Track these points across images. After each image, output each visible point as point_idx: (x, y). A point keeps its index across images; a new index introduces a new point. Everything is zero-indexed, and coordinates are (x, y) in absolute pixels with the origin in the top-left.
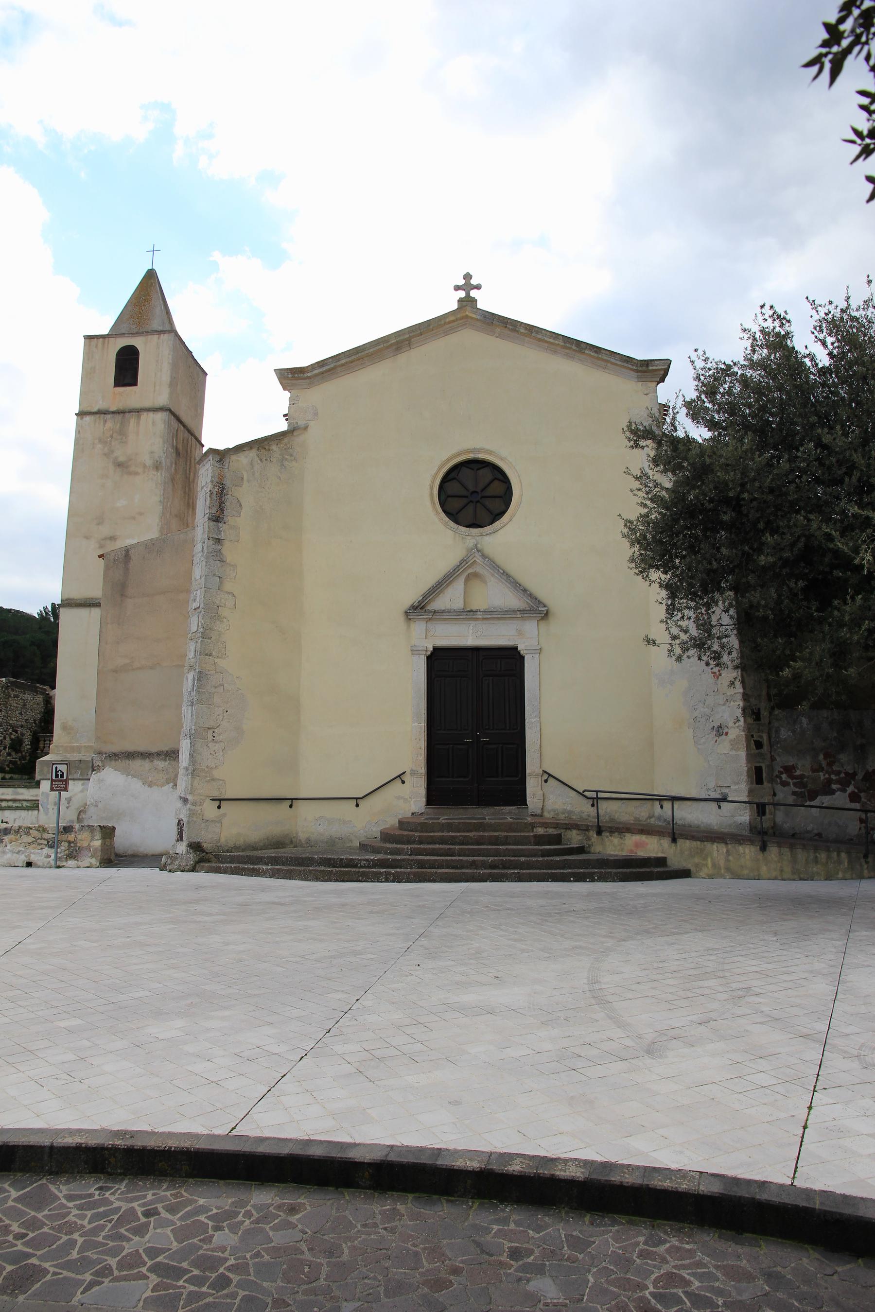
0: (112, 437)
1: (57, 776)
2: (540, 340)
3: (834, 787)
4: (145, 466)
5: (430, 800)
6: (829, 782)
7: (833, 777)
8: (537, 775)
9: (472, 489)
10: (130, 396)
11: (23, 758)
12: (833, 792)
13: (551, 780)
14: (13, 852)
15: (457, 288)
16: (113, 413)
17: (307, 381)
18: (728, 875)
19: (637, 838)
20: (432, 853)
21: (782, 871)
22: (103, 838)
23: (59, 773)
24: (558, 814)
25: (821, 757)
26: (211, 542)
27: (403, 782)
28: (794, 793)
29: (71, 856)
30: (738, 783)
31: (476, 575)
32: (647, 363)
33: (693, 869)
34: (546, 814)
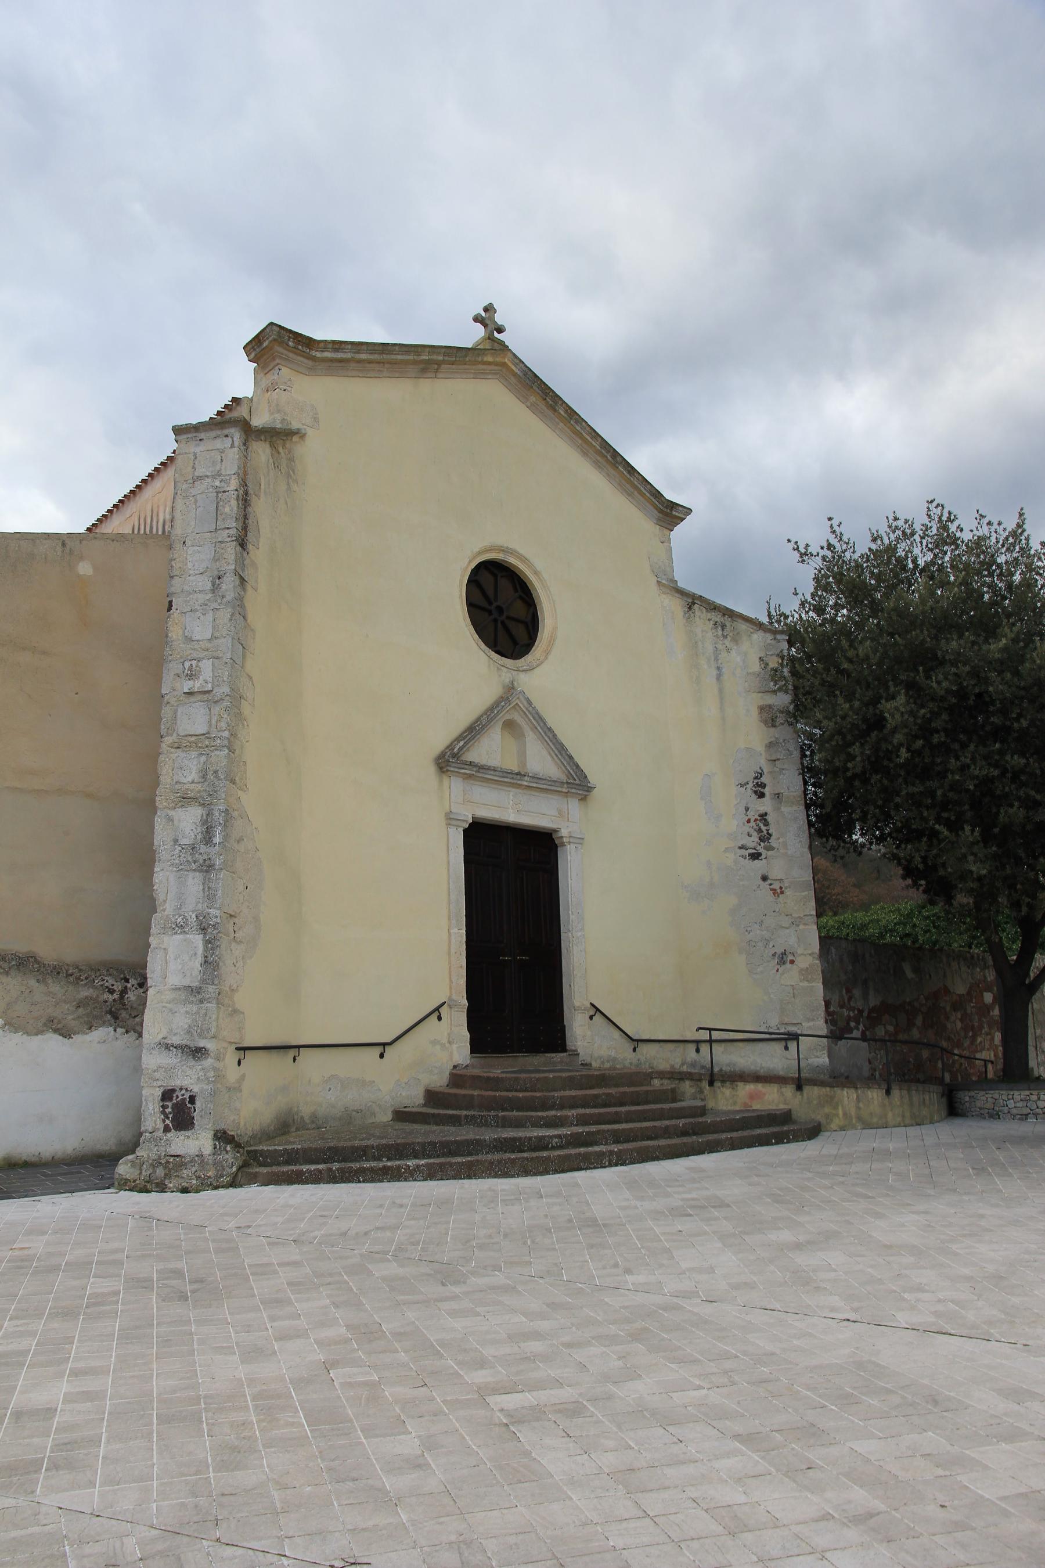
5: (477, 1046)
13: (598, 1018)
17: (310, 363)
18: (859, 1126)
19: (751, 1087)
20: (629, 1118)
21: (903, 1116)
30: (813, 1020)
32: (673, 505)
33: (823, 1121)
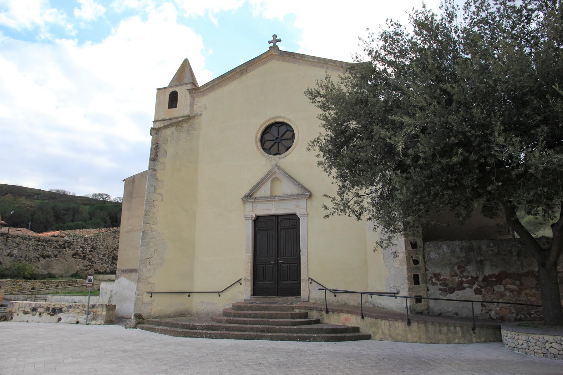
2: (306, 61)
3: (465, 285)
6: (462, 282)
7: (464, 279)
8: (306, 280)
9: (276, 136)
12: (464, 288)
13: (313, 283)
14: (72, 316)
15: (270, 42)
16: (167, 120)
18: (390, 339)
19: (346, 315)
21: (420, 337)
22: (108, 310)
24: (317, 301)
25: (456, 268)
26: (151, 171)
27: (241, 284)
28: (440, 289)
29: (94, 319)
31: (277, 179)
33: (372, 334)
34: (311, 301)
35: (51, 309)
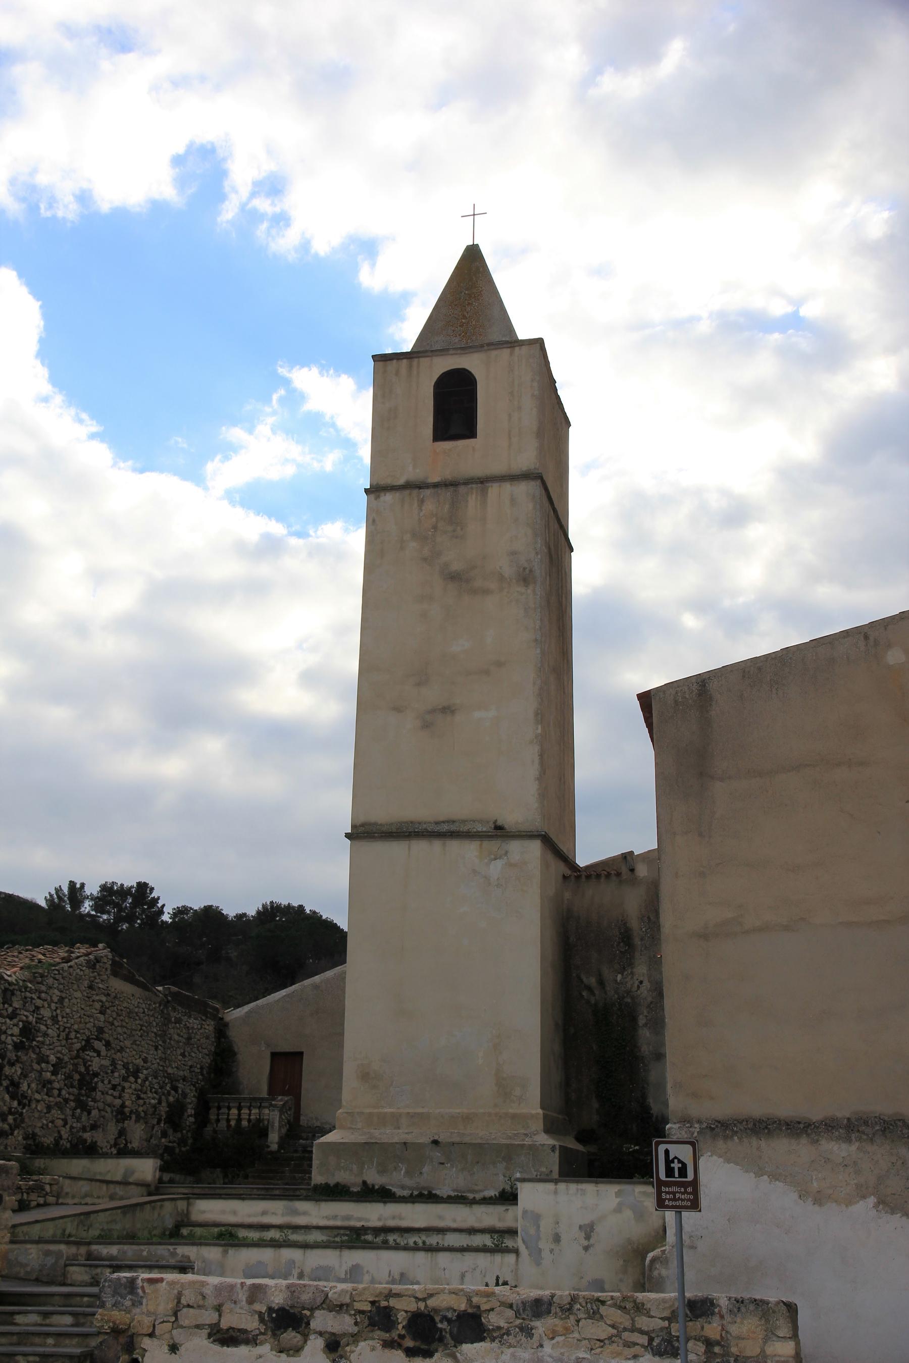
0: (435, 527)
1: (670, 1172)
4: (501, 578)
10: (463, 457)
11: (182, 1142)
16: (436, 486)
23: (676, 1166)
35: (402, 1317)
